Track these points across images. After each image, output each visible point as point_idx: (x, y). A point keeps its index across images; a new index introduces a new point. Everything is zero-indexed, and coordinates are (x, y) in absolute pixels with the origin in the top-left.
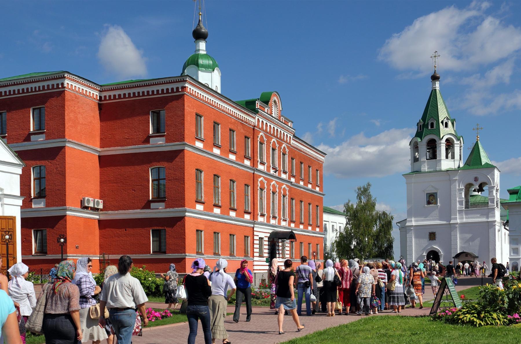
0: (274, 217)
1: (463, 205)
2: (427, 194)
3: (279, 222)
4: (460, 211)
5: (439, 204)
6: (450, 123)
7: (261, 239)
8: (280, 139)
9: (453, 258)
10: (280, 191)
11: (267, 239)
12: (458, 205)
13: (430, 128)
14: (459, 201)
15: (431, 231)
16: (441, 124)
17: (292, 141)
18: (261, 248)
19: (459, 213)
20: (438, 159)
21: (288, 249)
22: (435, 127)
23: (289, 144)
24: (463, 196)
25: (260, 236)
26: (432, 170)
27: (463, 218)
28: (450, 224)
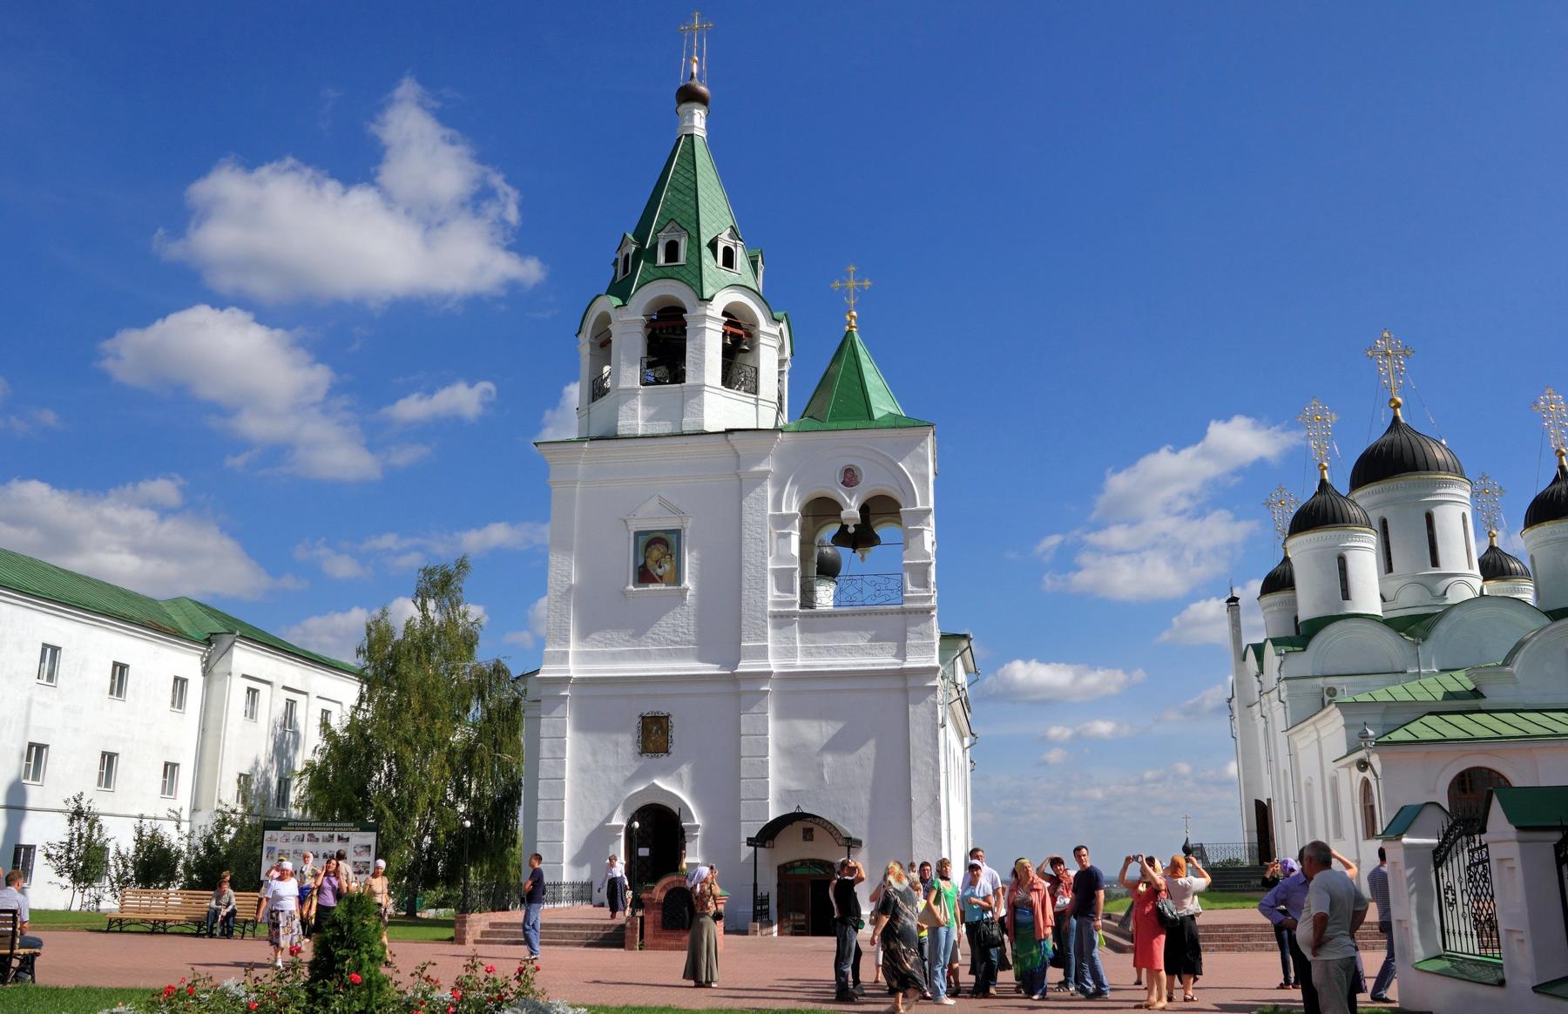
1: (792, 591)
2: (637, 534)
4: (782, 619)
5: (688, 583)
6: (740, 257)
9: (750, 842)
12: (772, 592)
13: (661, 260)
14: (776, 572)
15: (650, 708)
16: (706, 252)
19: (778, 627)
20: (689, 380)
22: (682, 259)
24: (795, 549)
26: (664, 427)
27: (790, 652)
28: (735, 679)
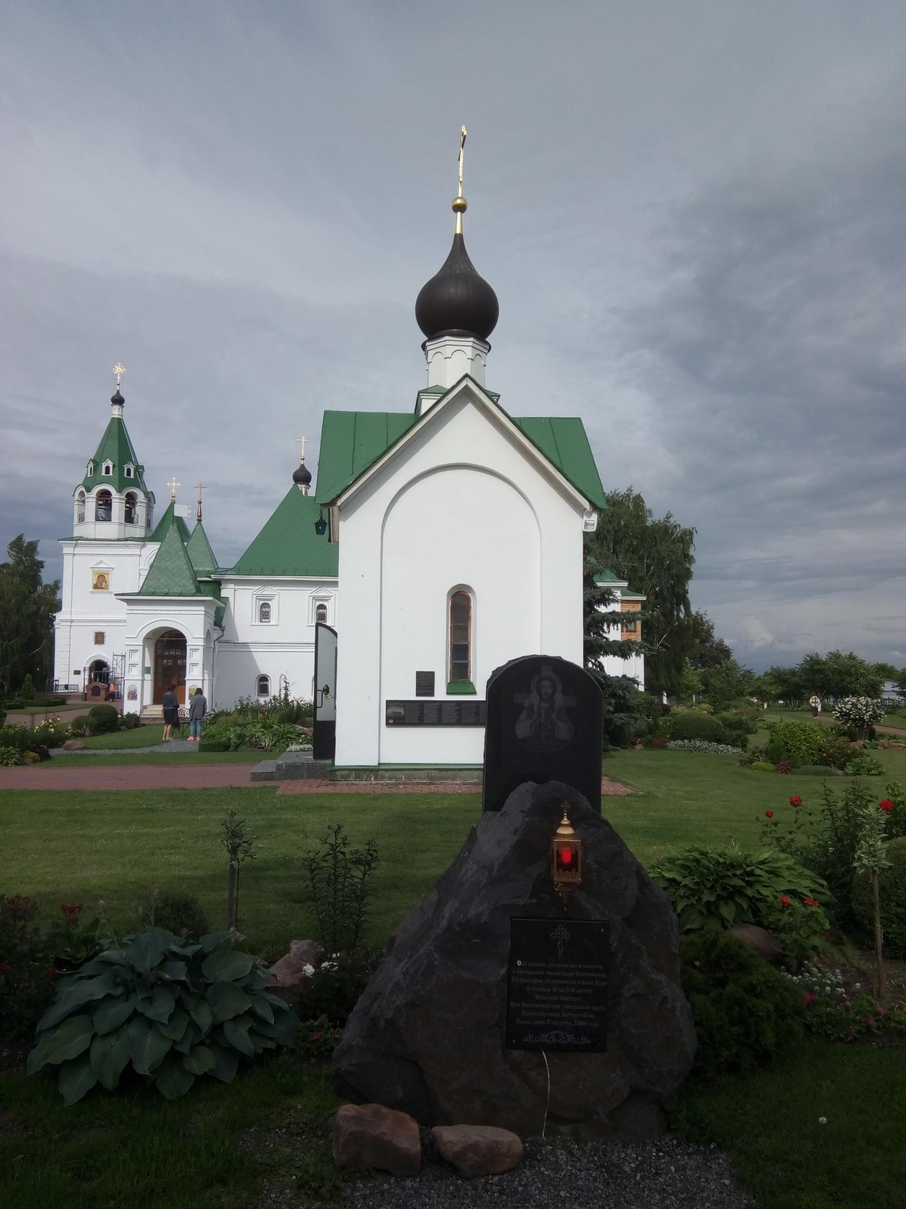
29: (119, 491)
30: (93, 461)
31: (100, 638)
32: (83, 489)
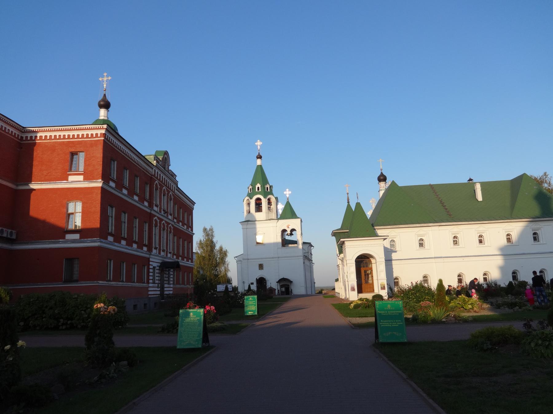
0: (163, 251)
3: (167, 255)
7: (154, 267)
8: (168, 187)
10: (167, 229)
11: (158, 268)
17: (176, 191)
18: (154, 276)
21: (172, 276)
23: (174, 192)
25: (154, 265)
29: (265, 197)
30: (251, 185)
31: (261, 267)
32: (247, 198)
